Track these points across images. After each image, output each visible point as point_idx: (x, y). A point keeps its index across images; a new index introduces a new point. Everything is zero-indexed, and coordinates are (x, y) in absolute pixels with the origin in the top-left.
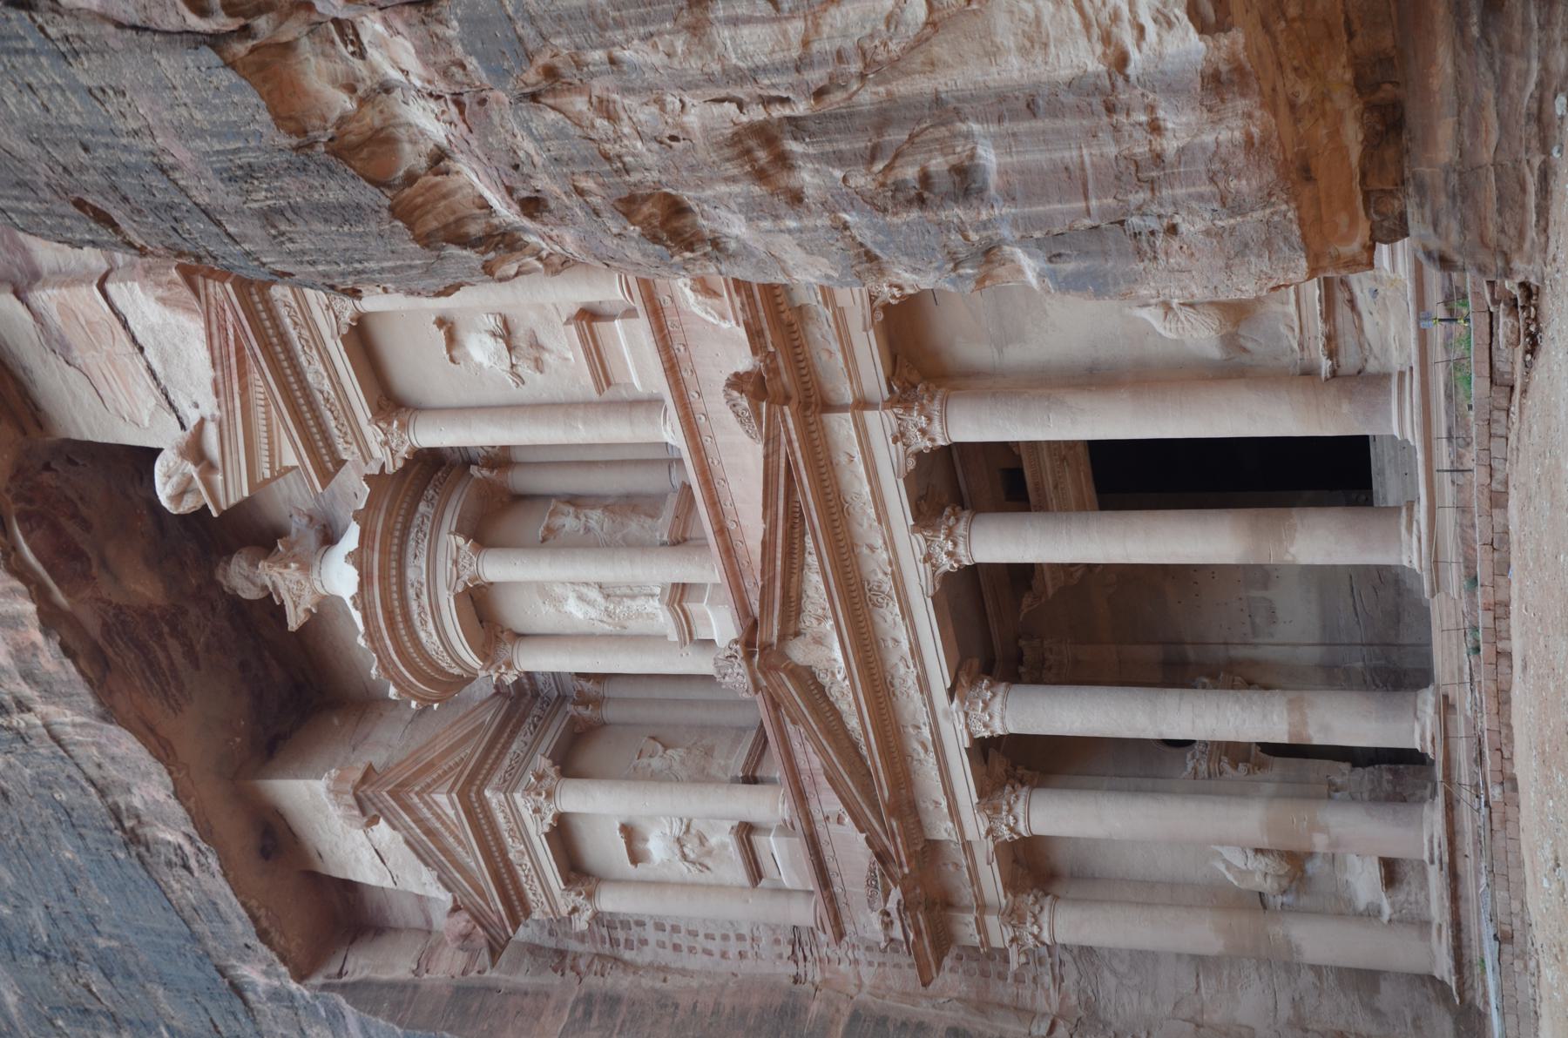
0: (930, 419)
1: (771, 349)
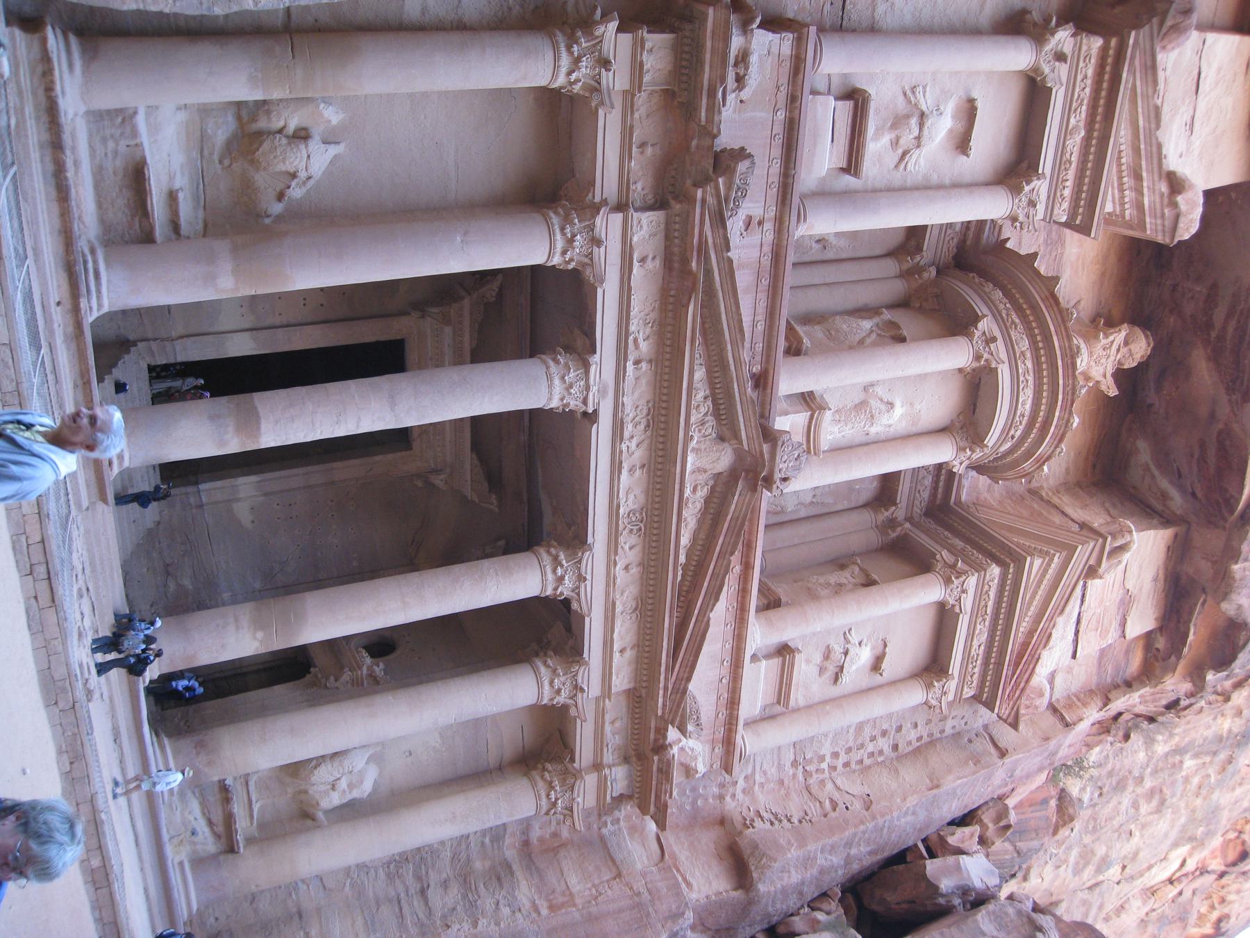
1: (656, 758)
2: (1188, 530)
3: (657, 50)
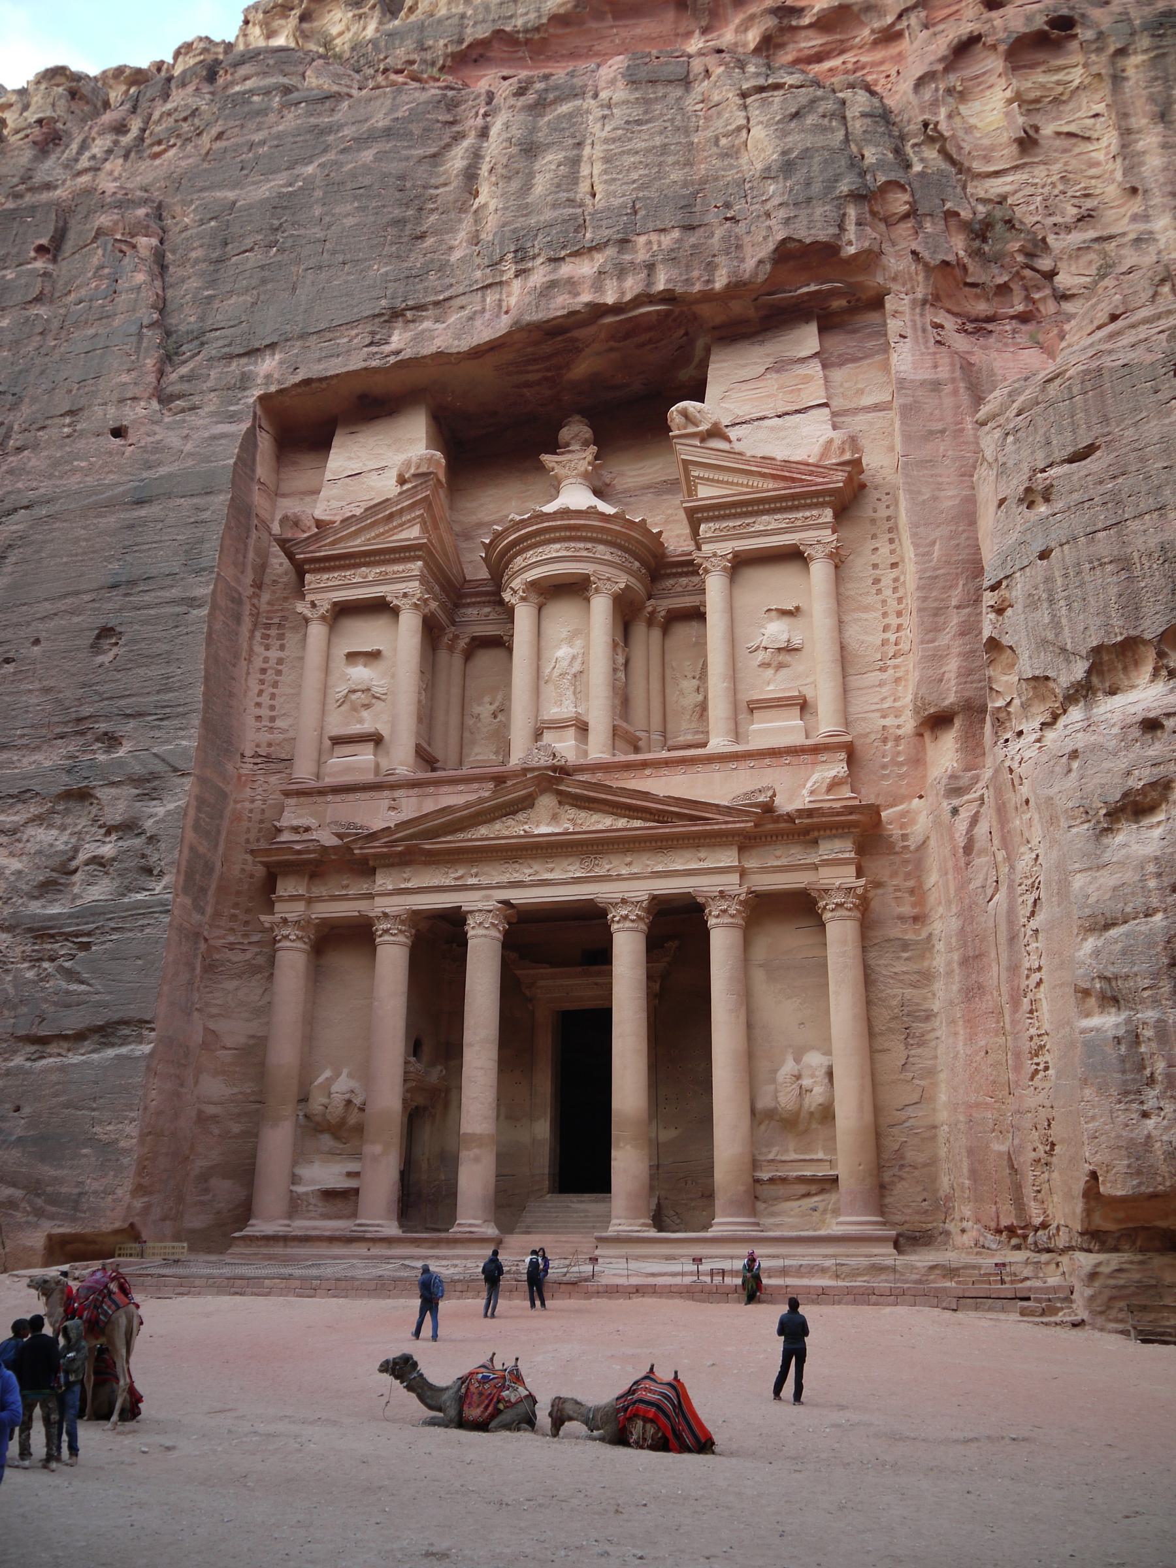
0: (733, 916)
2: (714, 328)
3: (287, 887)
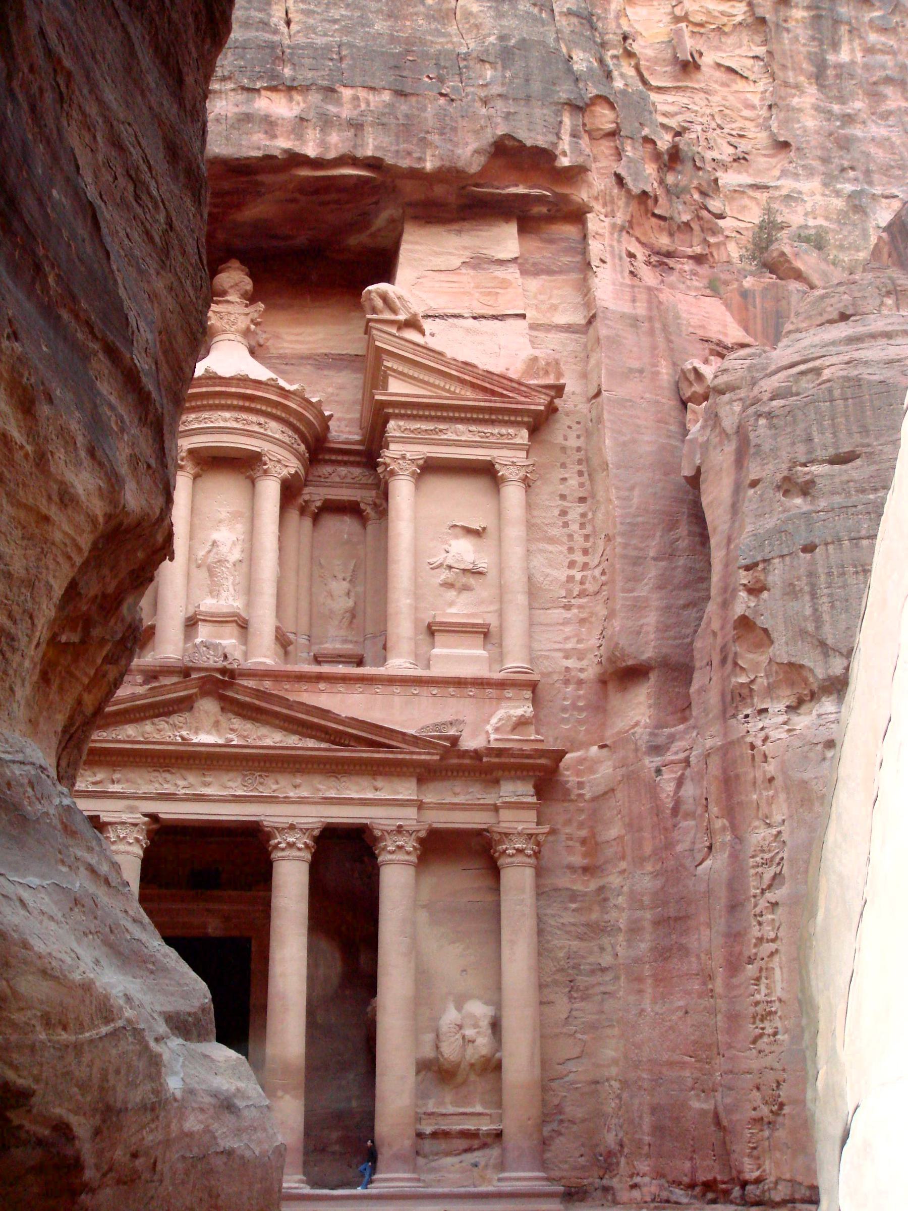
0: (408, 853)
